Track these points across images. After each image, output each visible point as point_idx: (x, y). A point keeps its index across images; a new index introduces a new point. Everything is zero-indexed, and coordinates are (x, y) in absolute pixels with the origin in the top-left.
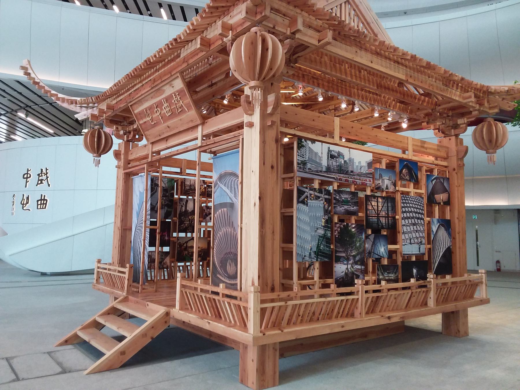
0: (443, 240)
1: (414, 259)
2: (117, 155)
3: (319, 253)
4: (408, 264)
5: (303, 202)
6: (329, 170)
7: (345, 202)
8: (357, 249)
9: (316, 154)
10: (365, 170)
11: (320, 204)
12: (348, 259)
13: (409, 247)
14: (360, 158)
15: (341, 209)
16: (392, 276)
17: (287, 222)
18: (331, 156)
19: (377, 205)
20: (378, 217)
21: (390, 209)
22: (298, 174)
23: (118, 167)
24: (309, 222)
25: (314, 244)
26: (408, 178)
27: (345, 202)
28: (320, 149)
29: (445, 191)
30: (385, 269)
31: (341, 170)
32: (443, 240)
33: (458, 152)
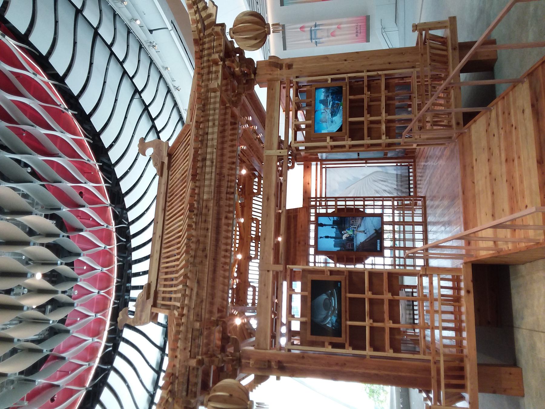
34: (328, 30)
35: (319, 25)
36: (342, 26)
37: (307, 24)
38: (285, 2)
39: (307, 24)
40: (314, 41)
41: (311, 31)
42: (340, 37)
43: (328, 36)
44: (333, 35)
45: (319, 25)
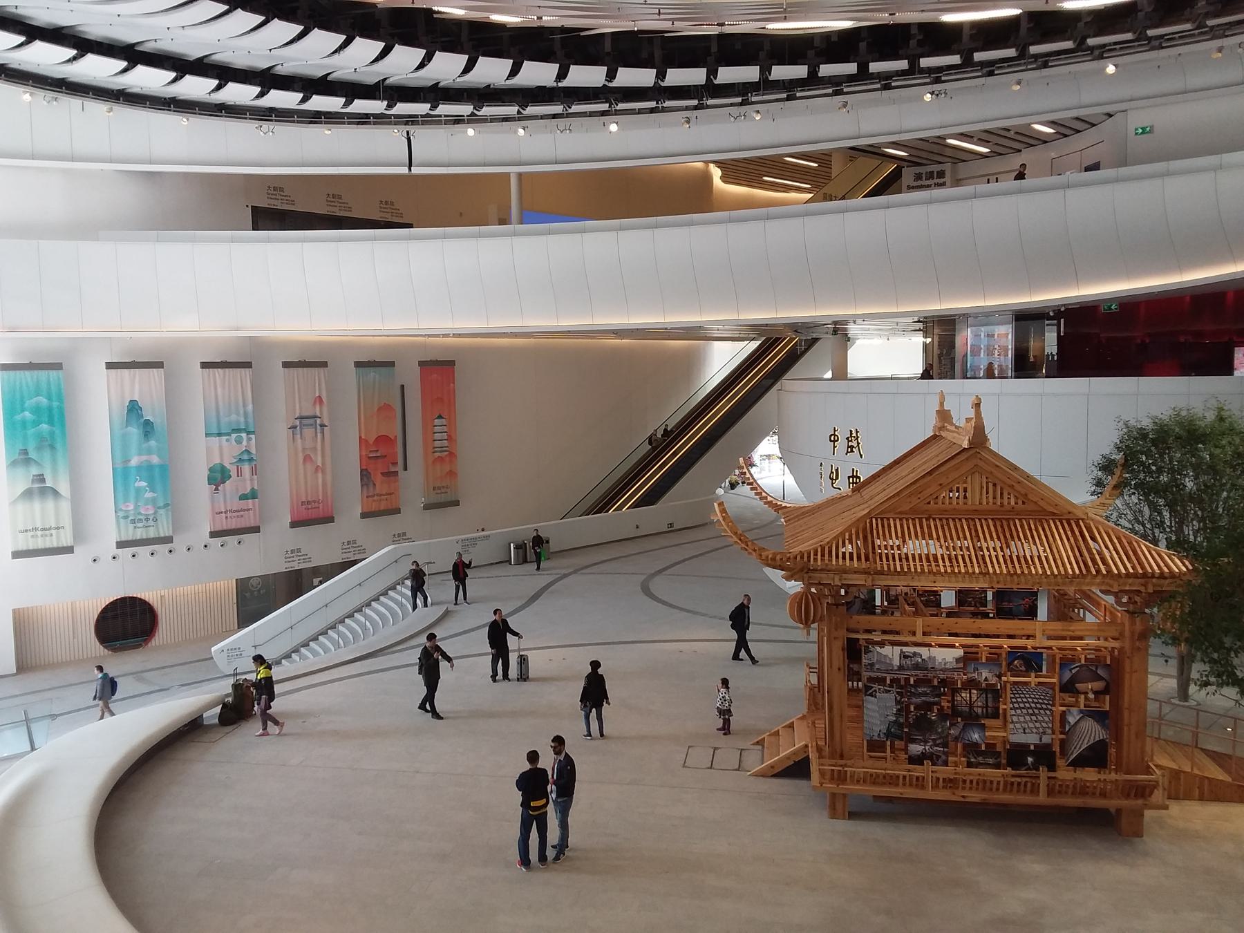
1: (1032, 747)
3: (888, 734)
5: (871, 695)
6: (901, 668)
7: (925, 694)
8: (938, 733)
9: (886, 656)
10: (954, 665)
11: (892, 696)
12: (926, 742)
15: (919, 700)
16: (991, 761)
18: (904, 656)
20: (971, 706)
21: (990, 700)
24: (879, 711)
25: (884, 728)
26: (1023, 668)
27: (925, 694)
28: (892, 654)
31: (916, 667)
32: (1090, 732)
33: (1132, 633)
34: (315, 449)
35: (323, 432)
36: (320, 475)
37: (325, 409)
38: (361, 369)
39: (325, 409)
40: (297, 422)
41: (315, 417)
42: (301, 471)
43: (304, 449)
44: (307, 458)
45: (323, 432)
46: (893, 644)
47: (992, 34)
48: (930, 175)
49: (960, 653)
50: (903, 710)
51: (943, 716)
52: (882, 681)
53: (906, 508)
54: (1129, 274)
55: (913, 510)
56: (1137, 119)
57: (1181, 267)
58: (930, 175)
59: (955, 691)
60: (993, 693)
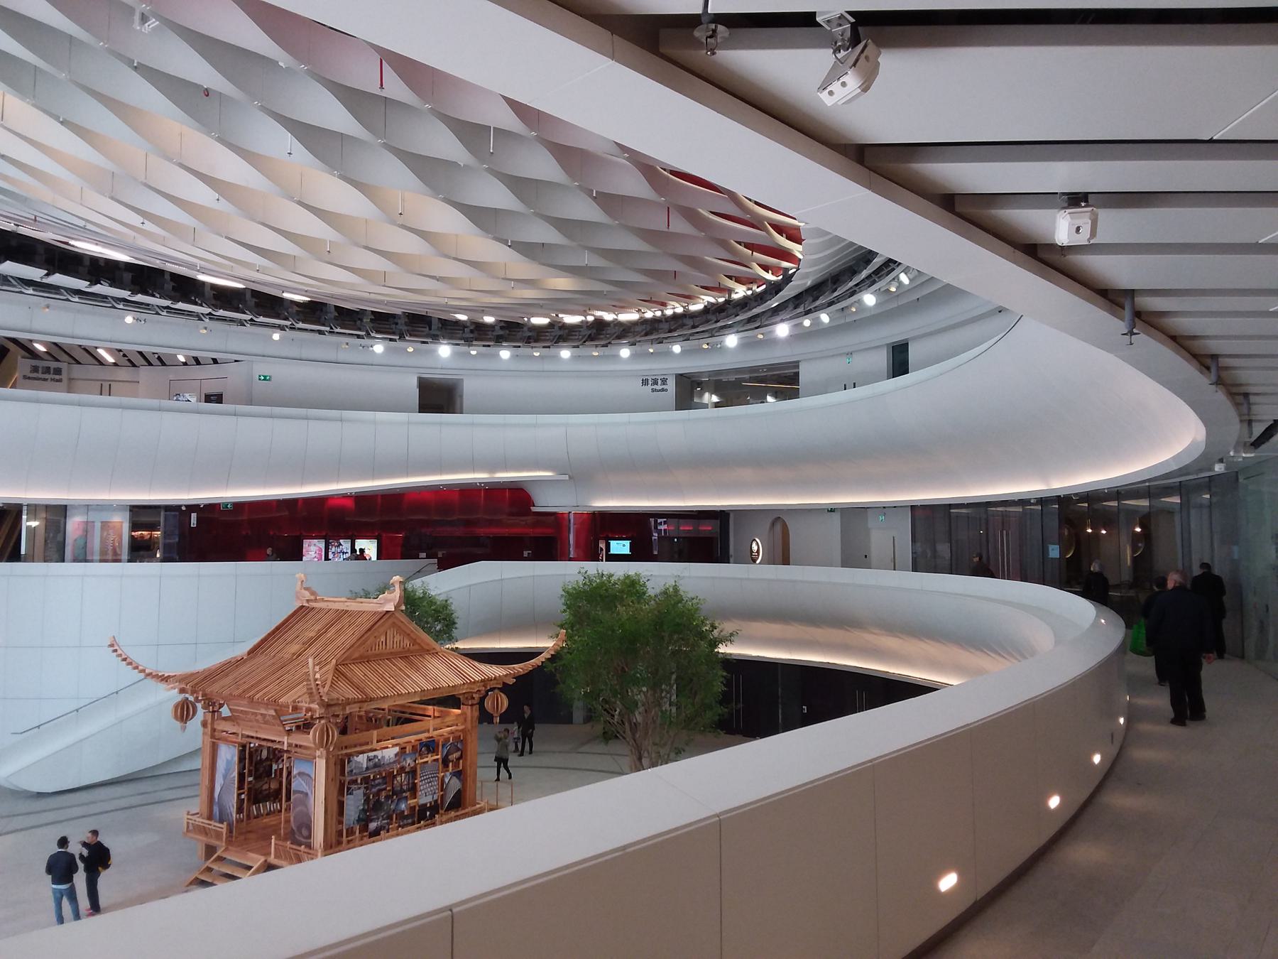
0: (455, 785)
2: (204, 724)
3: (359, 820)
4: (423, 808)
6: (367, 768)
13: (425, 798)
14: (389, 753)
15: (374, 790)
17: (341, 805)
18: (369, 760)
19: (402, 779)
22: (348, 779)
23: (204, 734)
24: (354, 803)
28: (362, 759)
29: (458, 750)
30: (406, 817)
31: (376, 766)
32: (455, 785)
46: (363, 752)
47: (225, 298)
48: (47, 370)
49: (397, 749)
50: (367, 801)
51: (387, 797)
52: (355, 782)
53: (356, 655)
54: (265, 483)
55: (361, 657)
56: (261, 368)
57: (303, 482)
58: (47, 370)
59: (395, 777)
60: (413, 772)
